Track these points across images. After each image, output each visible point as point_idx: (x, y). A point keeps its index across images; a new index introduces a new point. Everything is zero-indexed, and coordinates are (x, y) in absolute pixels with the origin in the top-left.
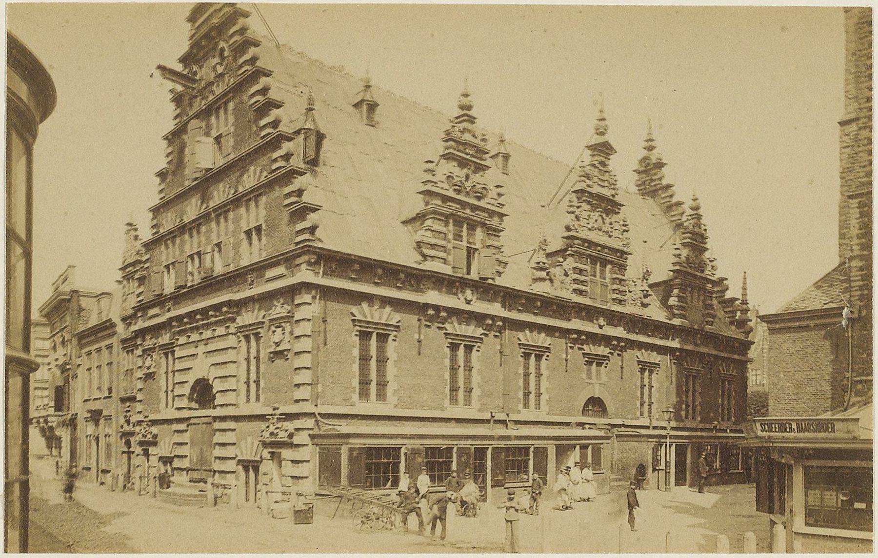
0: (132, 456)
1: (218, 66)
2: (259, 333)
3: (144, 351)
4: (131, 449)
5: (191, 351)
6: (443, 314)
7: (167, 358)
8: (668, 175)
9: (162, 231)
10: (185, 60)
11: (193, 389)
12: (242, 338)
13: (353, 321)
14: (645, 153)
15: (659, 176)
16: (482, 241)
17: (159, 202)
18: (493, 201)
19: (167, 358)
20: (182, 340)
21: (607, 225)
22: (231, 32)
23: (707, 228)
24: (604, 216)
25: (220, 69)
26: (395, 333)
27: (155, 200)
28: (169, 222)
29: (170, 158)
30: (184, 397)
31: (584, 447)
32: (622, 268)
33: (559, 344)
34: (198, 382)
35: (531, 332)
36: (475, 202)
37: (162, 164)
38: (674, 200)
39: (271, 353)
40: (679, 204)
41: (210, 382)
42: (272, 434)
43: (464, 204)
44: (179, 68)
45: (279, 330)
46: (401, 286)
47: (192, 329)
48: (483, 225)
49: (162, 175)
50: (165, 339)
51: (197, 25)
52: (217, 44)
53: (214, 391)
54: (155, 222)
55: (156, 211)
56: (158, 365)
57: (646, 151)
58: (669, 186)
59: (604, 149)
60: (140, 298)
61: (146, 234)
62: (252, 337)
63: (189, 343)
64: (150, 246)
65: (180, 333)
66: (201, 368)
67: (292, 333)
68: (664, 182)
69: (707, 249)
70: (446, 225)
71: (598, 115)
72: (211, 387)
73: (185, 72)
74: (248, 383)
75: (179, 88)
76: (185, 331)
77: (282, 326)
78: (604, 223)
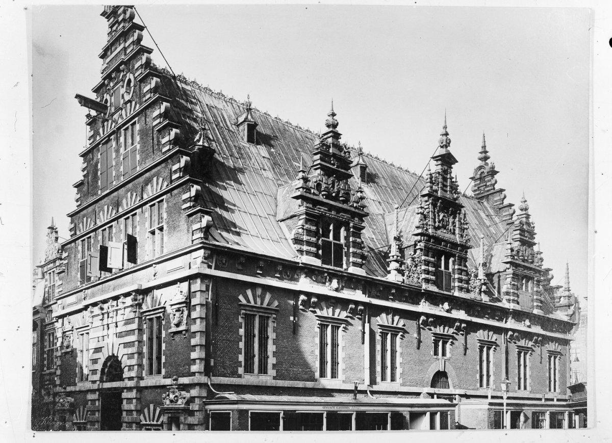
1: (125, 95)
8: (501, 181)
10: (97, 90)
11: (105, 364)
14: (480, 163)
15: (493, 182)
17: (77, 208)
18: (355, 205)
22: (136, 66)
23: (534, 225)
25: (127, 98)
26: (275, 316)
27: (73, 207)
29: (85, 172)
32: (463, 260)
33: (411, 325)
34: (109, 358)
35: (387, 314)
36: (340, 205)
37: (79, 177)
38: (506, 202)
40: (511, 205)
41: (119, 359)
42: (171, 401)
43: (331, 208)
44: (93, 96)
45: (178, 314)
49: (79, 186)
51: (108, 60)
52: (125, 76)
53: (123, 366)
54: (73, 226)
57: (480, 162)
58: (501, 191)
59: (447, 160)
60: (61, 289)
61: (65, 235)
67: (189, 315)
68: (497, 187)
69: (535, 244)
72: (120, 363)
73: (98, 100)
74: (150, 359)
75: (93, 113)
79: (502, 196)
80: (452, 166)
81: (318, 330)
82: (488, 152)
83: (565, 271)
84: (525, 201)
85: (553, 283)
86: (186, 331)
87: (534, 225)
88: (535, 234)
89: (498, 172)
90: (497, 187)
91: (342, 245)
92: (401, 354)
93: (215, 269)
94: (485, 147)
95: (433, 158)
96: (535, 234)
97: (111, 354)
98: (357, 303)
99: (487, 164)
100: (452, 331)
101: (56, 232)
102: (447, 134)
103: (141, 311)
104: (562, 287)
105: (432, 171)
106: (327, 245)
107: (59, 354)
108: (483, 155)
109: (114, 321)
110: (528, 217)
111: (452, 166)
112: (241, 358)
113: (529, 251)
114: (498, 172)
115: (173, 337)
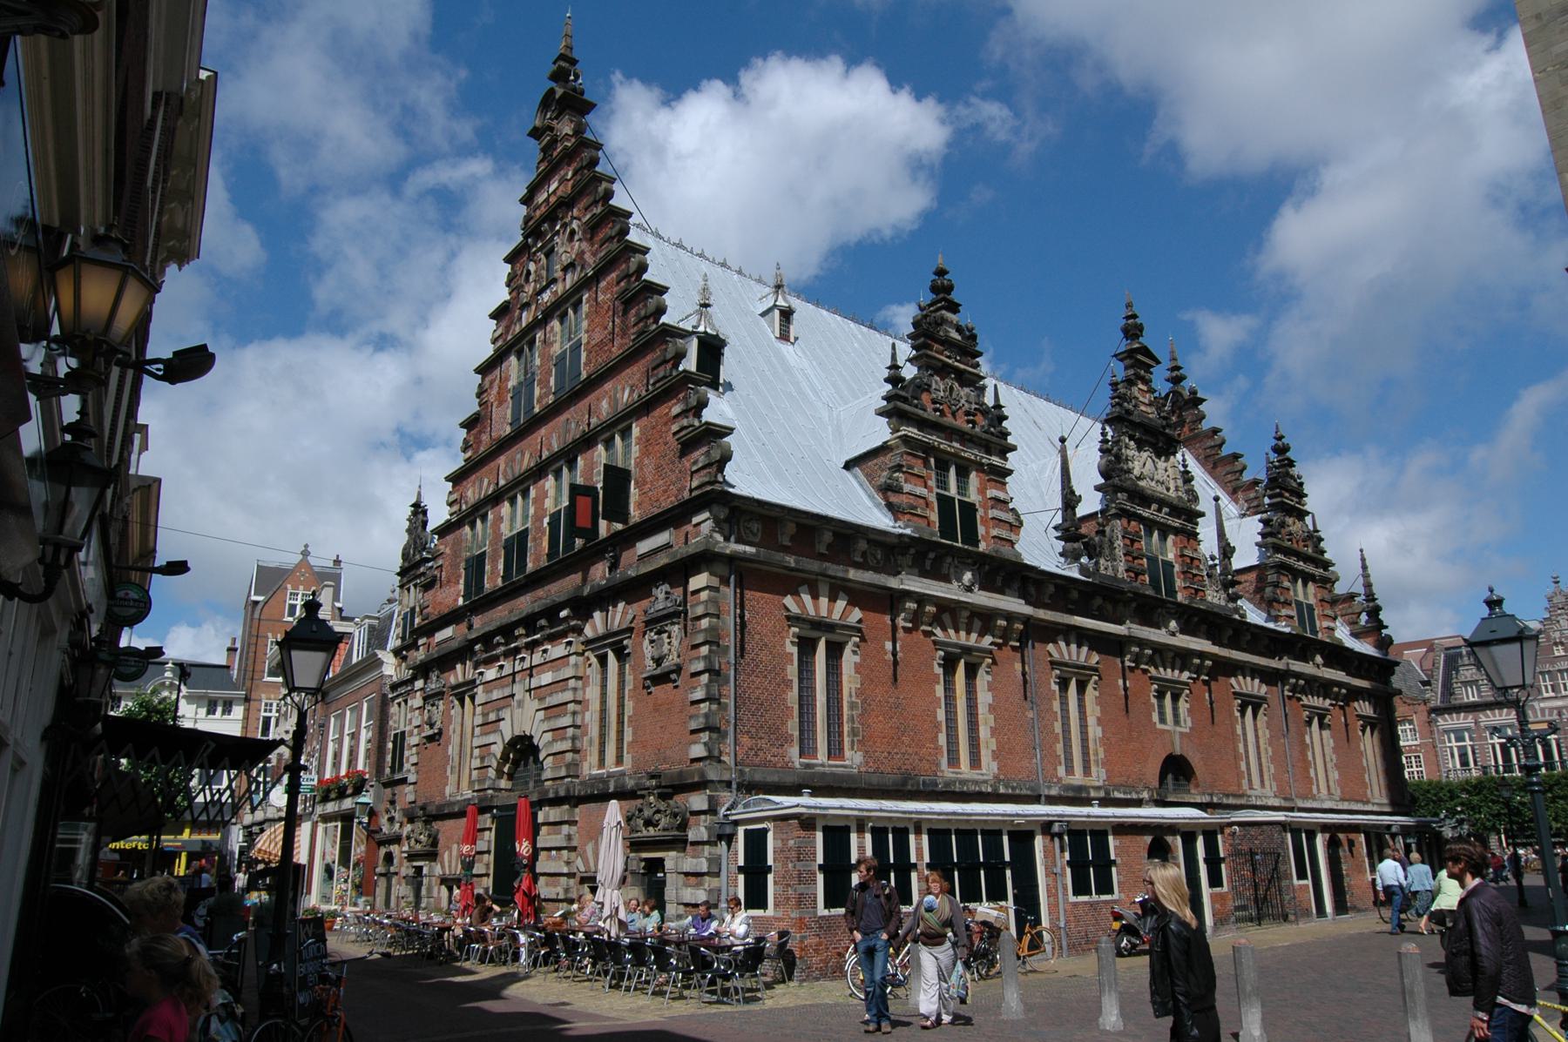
0: (394, 880)
2: (625, 648)
3: (425, 699)
4: (392, 869)
5: (507, 692)
6: (930, 609)
7: (462, 704)
9: (464, 507)
11: (505, 757)
12: (594, 660)
13: (788, 618)
16: (982, 491)
19: (462, 704)
20: (491, 674)
21: (1161, 471)
28: (474, 492)
30: (490, 769)
31: (1189, 839)
39: (645, 679)
46: (861, 560)
47: (506, 655)
48: (980, 467)
50: (459, 674)
55: (457, 479)
56: (446, 716)
62: (611, 657)
63: (502, 678)
64: (444, 530)
65: (489, 662)
66: (526, 718)
70: (926, 464)
71: (1125, 312)
76: (496, 659)
77: (666, 631)
78: (1156, 469)
81: (939, 671)
83: (1359, 564)
86: (678, 669)
88: (1306, 495)
90: (1205, 425)
91: (974, 505)
93: (736, 542)
95: (1115, 356)
96: (1306, 495)
97: (517, 733)
98: (1010, 617)
100: (1185, 676)
101: (425, 513)
102: (1134, 316)
103: (582, 639)
105: (1119, 379)
106: (945, 503)
107: (414, 740)
109: (527, 665)
112: (792, 726)
113: (1294, 526)
115: (648, 687)
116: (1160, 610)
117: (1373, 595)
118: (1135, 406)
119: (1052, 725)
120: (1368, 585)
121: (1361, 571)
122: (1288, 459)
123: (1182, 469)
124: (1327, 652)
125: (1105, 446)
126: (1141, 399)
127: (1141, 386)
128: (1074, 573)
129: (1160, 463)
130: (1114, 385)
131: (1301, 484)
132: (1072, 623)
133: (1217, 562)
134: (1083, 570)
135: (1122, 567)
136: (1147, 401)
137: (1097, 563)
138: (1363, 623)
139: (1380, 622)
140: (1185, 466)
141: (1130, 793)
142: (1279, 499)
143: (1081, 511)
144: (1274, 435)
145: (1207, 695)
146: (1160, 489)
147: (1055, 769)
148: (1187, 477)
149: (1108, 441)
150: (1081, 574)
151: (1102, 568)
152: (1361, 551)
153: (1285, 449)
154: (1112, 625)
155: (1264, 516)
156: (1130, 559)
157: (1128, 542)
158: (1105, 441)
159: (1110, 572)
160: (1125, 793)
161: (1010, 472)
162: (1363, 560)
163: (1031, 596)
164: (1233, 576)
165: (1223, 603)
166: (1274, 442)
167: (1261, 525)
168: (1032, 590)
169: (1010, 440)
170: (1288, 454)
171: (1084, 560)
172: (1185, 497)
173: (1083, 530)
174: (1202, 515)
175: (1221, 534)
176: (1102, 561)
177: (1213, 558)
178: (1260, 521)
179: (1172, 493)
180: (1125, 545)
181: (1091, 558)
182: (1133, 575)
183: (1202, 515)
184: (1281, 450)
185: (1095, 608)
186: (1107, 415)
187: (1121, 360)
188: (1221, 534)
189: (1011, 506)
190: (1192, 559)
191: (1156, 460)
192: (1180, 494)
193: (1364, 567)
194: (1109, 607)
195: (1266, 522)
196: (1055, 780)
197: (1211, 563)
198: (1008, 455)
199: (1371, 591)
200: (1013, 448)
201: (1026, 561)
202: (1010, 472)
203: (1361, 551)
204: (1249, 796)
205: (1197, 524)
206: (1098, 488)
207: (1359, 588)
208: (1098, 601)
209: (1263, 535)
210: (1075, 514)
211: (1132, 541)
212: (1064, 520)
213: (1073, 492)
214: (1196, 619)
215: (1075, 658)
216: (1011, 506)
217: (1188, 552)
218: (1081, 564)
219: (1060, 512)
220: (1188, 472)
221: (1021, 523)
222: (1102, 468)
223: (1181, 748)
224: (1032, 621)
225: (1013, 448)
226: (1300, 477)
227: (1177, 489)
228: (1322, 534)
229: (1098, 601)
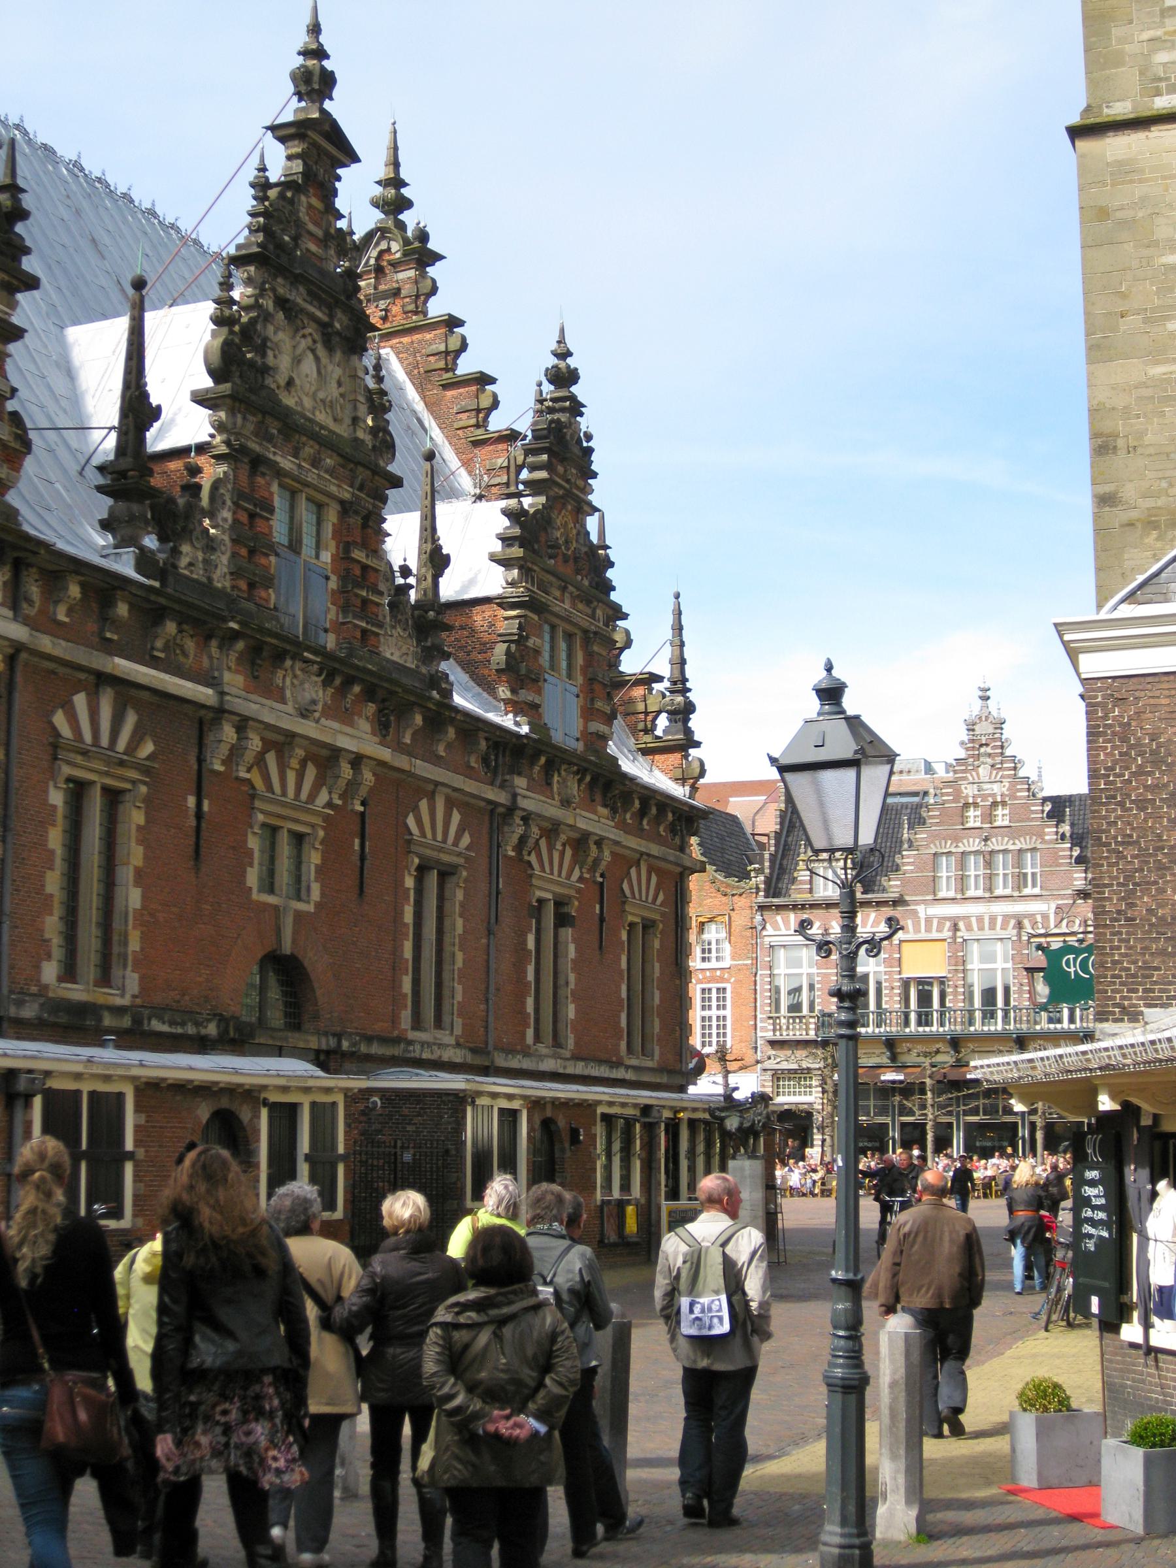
23: (590, 444)
24: (321, 351)
79: (454, 343)
80: (339, 171)
82: (405, 185)
83: (669, 620)
84: (569, 354)
85: (630, 663)
87: (590, 444)
88: (594, 475)
89: (440, 257)
90: (436, 308)
92: (138, 872)
94: (396, 164)
96: (594, 475)
99: (401, 226)
104: (660, 679)
108: (391, 192)
110: (576, 408)
111: (339, 171)
114: (440, 257)
116: (288, 663)
117: (684, 680)
118: (296, 239)
119: (42, 876)
120: (680, 662)
121: (668, 634)
122: (573, 398)
123: (371, 383)
124: (588, 778)
125: (227, 312)
126: (311, 227)
127: (314, 201)
128: (125, 566)
129: (330, 368)
130: (261, 186)
131: (590, 450)
132: (108, 669)
133: (412, 580)
134: (144, 561)
135: (223, 560)
136: (319, 233)
137: (175, 552)
138: (659, 732)
139: (688, 732)
140: (380, 379)
141: (183, 1024)
142: (542, 474)
143: (159, 439)
144: (554, 346)
145: (357, 841)
146: (322, 417)
147: (37, 968)
148: (379, 402)
149: (232, 302)
150: (139, 569)
151: (184, 562)
152: (677, 596)
153: (572, 377)
154: (189, 685)
155: (513, 502)
156: (244, 552)
157: (244, 517)
158: (225, 302)
159: (198, 574)
160: (172, 1023)
161: (17, 333)
162: (678, 613)
163: (30, 602)
164: (438, 613)
165: (411, 664)
166: (552, 361)
167: (506, 522)
168: (34, 590)
169: (29, 264)
170: (574, 389)
171: (150, 542)
172: (367, 438)
173: (156, 481)
174: (397, 482)
175: (429, 530)
176: (186, 548)
177: (405, 571)
178: (506, 513)
179: (343, 430)
180: (236, 521)
181: (162, 539)
182: (243, 585)
183: (397, 482)
184: (563, 377)
185: (159, 644)
186: (239, 247)
187: (282, 140)
188: (429, 530)
189: (11, 406)
190: (365, 568)
191: (324, 360)
192: (360, 434)
193: (678, 628)
194: (190, 645)
195: (515, 516)
196: (34, 989)
197: (400, 581)
198: (19, 296)
199: (683, 672)
200: (31, 283)
201: (26, 528)
202: (17, 333)
203: (677, 596)
204: (410, 1042)
205: (384, 500)
206: (200, 399)
207: (663, 668)
208: (171, 627)
209: (505, 540)
210: (141, 441)
211: (252, 516)
212: (120, 450)
213: (145, 396)
214: (357, 689)
215: (105, 741)
216: (11, 406)
217: (358, 555)
218: (142, 549)
219: (113, 436)
220: (383, 393)
221: (27, 445)
222: (216, 359)
223: (294, 941)
224: (24, 656)
225: (31, 283)
226: (589, 437)
227: (355, 420)
228: (613, 555)
229: (171, 627)
